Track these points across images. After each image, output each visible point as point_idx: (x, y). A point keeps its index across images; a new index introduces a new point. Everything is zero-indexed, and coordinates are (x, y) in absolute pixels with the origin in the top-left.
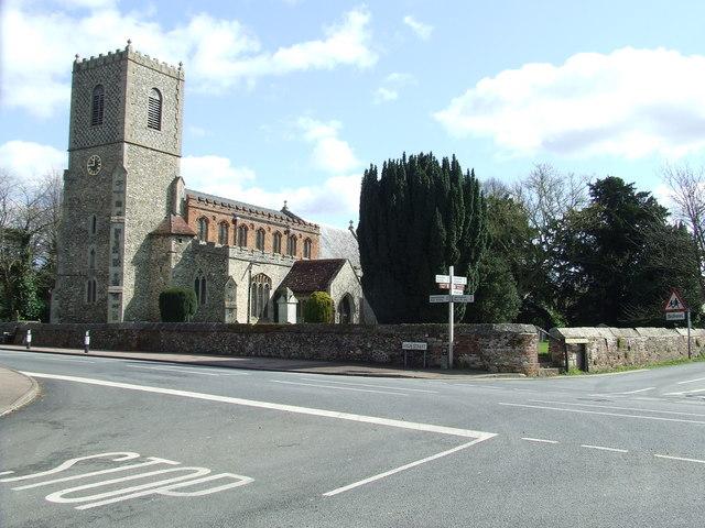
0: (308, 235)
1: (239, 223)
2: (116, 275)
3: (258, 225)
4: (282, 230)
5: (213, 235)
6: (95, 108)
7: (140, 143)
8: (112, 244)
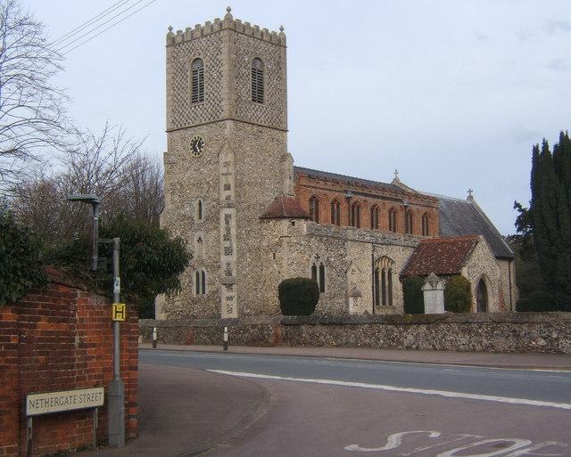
0: (427, 210)
1: (352, 202)
2: (228, 264)
4: (397, 205)
5: (325, 213)
6: (194, 83)
8: (223, 231)
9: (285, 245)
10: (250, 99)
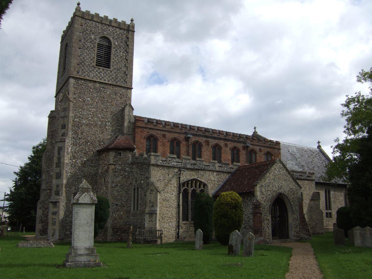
0: (268, 150)
3: (213, 142)
7: (88, 78)
8: (55, 160)
9: (110, 171)
10: (95, 64)
